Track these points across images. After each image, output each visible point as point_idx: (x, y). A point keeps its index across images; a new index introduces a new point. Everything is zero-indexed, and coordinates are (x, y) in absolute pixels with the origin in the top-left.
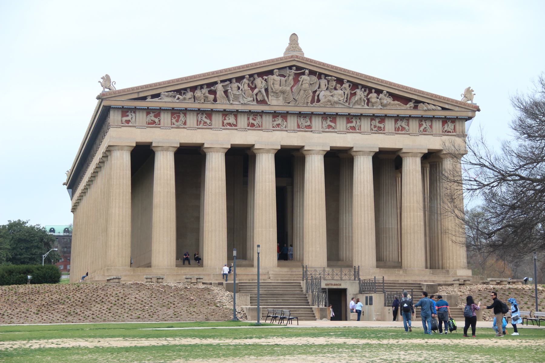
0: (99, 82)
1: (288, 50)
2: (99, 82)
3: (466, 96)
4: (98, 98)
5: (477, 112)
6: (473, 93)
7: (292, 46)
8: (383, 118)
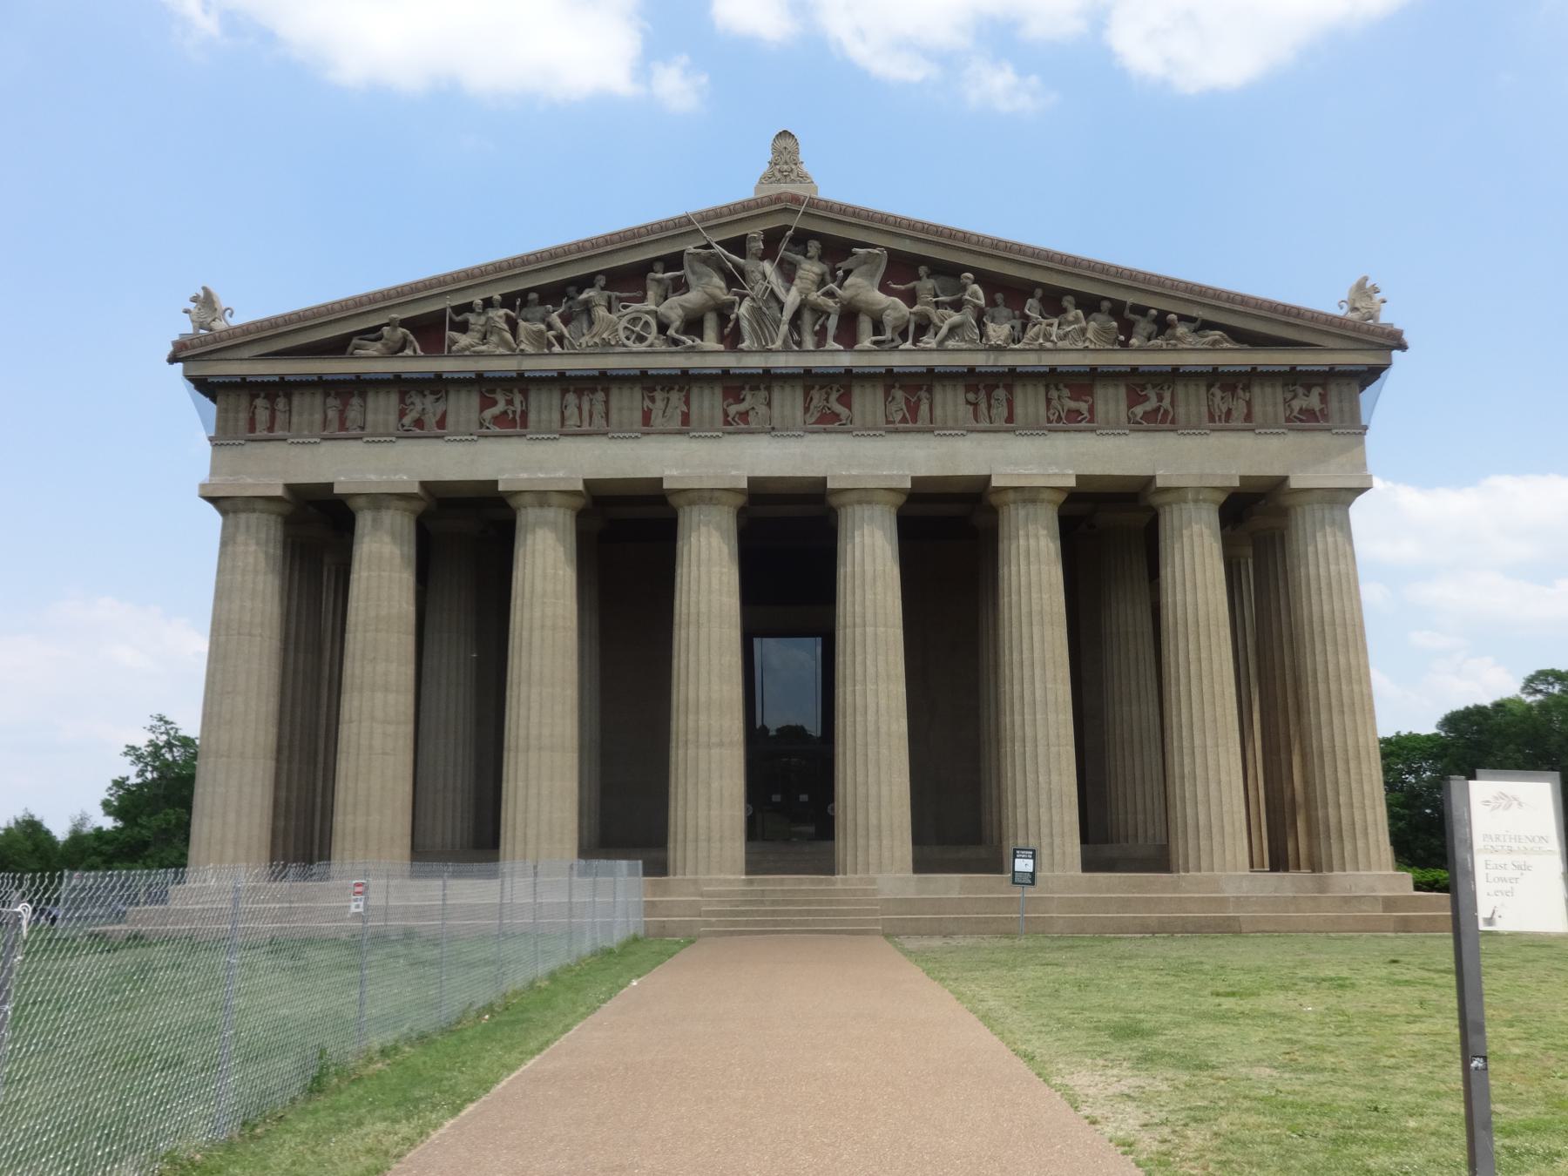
0: (186, 311)
1: (767, 179)
2: (186, 311)
3: (1357, 305)
4: (173, 359)
5: (1396, 354)
6: (1378, 297)
7: (778, 167)
8: (1084, 381)
